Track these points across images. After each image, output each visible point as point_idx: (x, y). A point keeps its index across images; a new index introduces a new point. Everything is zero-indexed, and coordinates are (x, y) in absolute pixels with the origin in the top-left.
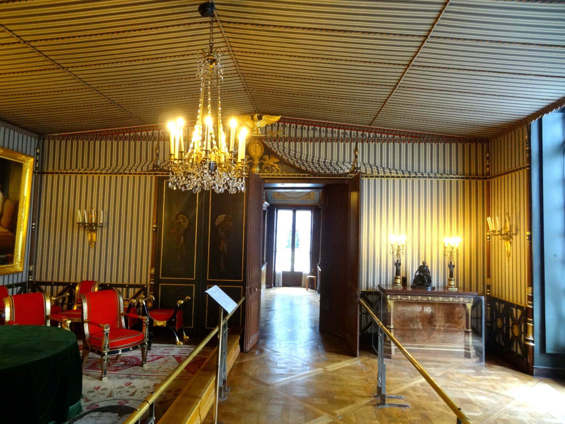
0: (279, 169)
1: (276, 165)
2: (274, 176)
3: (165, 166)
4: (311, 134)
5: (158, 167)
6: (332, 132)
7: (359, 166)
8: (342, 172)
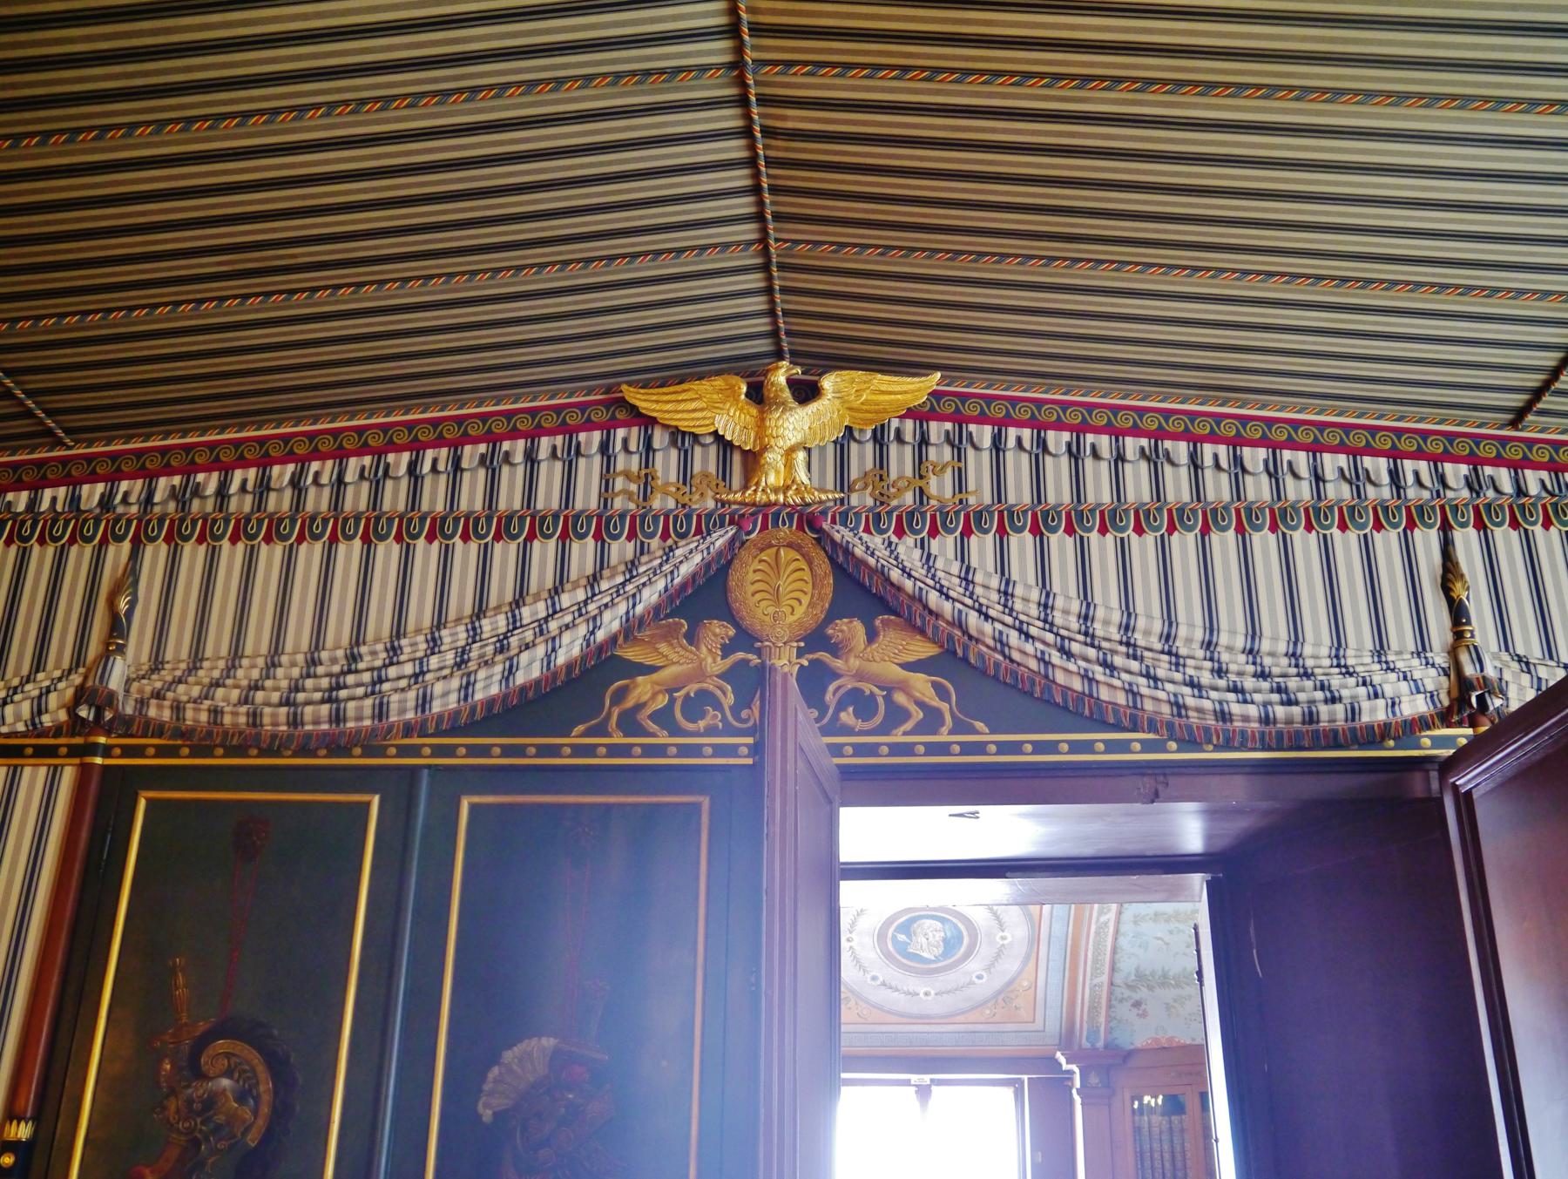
0: (936, 702)
1: (922, 684)
2: (908, 749)
3: (158, 695)
5: (112, 696)
7: (1490, 672)
8: (1381, 716)
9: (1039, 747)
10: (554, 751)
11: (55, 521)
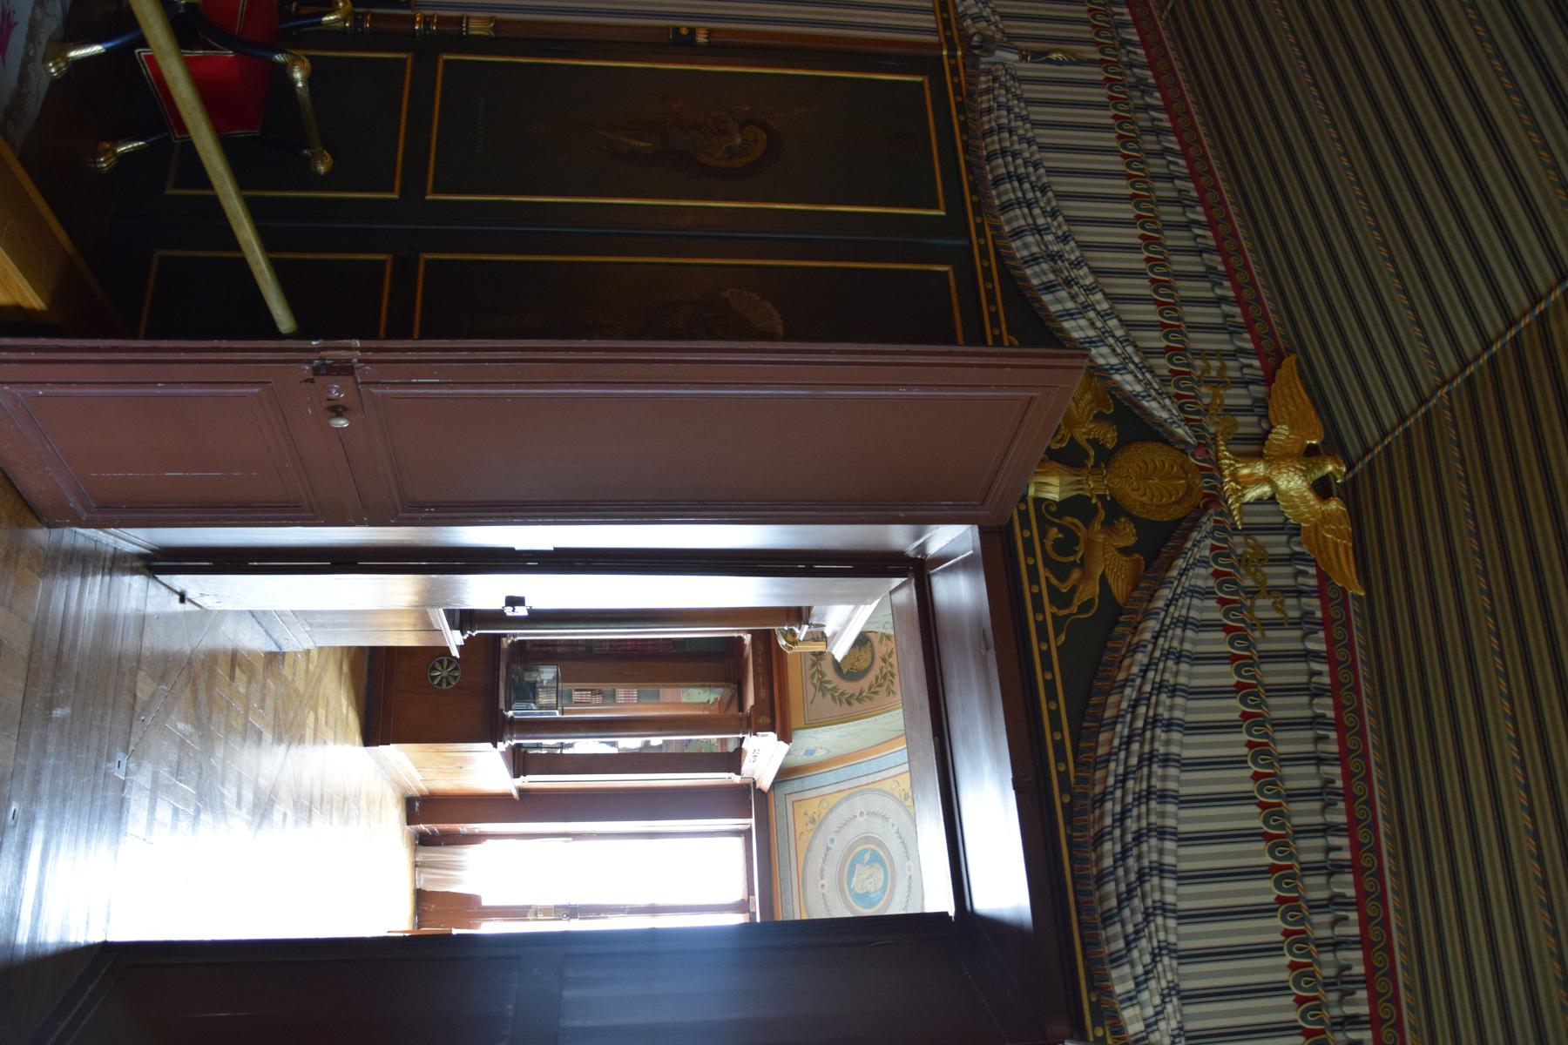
0: (1076, 602)
1: (1091, 590)
3: (995, 79)
4: (1300, 777)
6: (1335, 901)
8: (1119, 989)
9: (1055, 715)
11: (1107, 16)
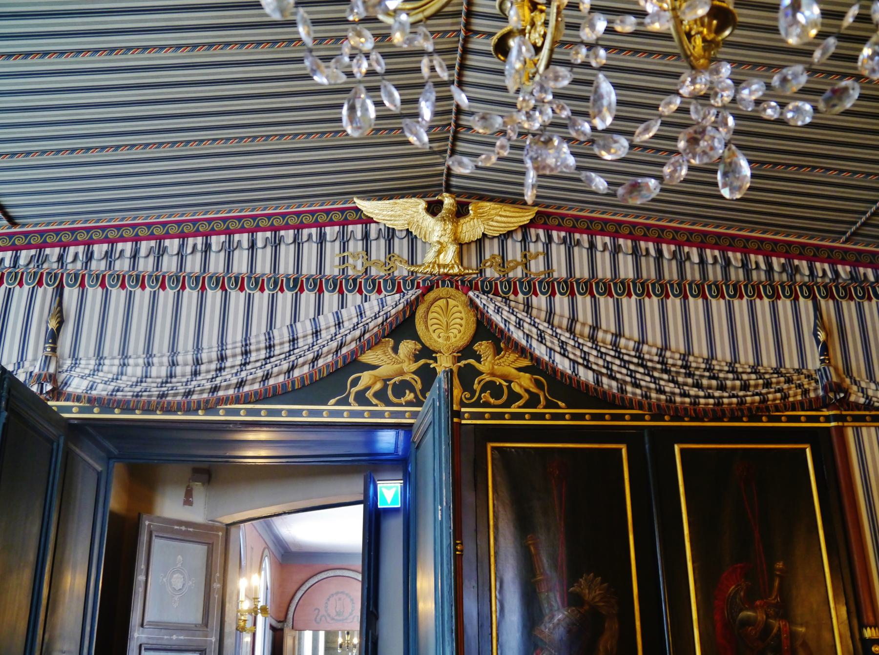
0: (534, 390)
2: (521, 416)
10: (319, 413)
